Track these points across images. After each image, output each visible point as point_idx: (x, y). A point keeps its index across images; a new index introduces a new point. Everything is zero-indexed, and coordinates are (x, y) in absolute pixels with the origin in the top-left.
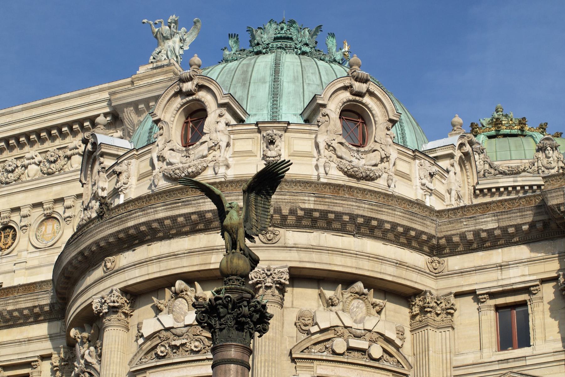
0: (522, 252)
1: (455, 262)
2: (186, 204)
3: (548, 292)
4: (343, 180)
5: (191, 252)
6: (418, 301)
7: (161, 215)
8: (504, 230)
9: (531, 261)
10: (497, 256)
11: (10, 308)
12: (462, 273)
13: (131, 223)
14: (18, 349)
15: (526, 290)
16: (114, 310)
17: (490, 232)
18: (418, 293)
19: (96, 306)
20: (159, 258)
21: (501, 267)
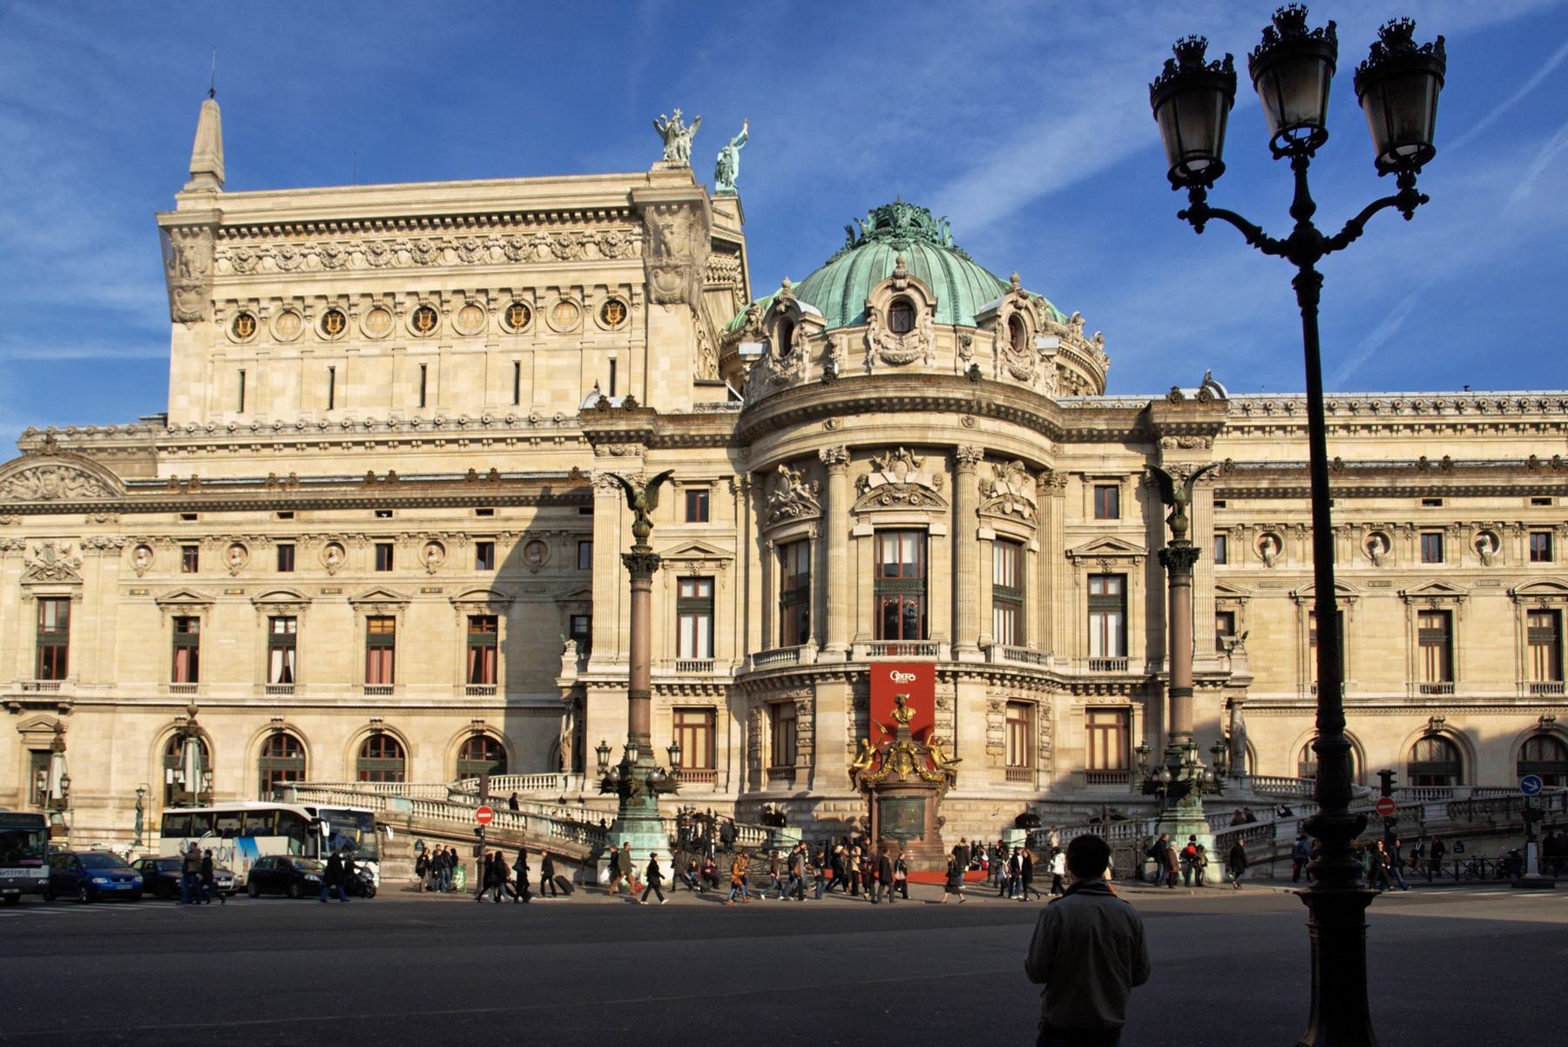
0: (1120, 449)
1: (1069, 448)
2: (913, 389)
3: (1134, 481)
4: (1006, 378)
5: (912, 427)
6: (1044, 476)
7: (890, 394)
8: (1111, 431)
9: (1125, 457)
10: (1101, 449)
11: (693, 433)
12: (1074, 458)
13: (863, 396)
14: (698, 468)
15: (1120, 478)
16: (839, 462)
17: (1100, 431)
18: (1045, 469)
19: (822, 455)
20: (885, 428)
21: (1103, 458)
